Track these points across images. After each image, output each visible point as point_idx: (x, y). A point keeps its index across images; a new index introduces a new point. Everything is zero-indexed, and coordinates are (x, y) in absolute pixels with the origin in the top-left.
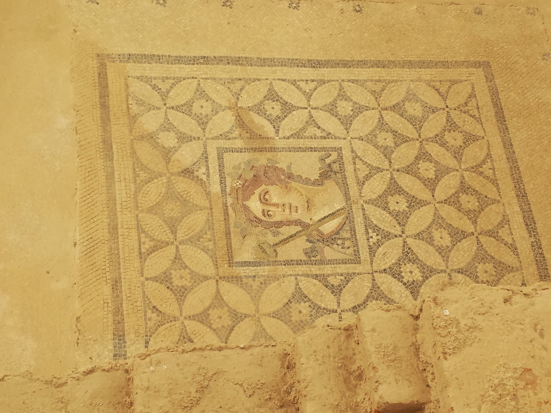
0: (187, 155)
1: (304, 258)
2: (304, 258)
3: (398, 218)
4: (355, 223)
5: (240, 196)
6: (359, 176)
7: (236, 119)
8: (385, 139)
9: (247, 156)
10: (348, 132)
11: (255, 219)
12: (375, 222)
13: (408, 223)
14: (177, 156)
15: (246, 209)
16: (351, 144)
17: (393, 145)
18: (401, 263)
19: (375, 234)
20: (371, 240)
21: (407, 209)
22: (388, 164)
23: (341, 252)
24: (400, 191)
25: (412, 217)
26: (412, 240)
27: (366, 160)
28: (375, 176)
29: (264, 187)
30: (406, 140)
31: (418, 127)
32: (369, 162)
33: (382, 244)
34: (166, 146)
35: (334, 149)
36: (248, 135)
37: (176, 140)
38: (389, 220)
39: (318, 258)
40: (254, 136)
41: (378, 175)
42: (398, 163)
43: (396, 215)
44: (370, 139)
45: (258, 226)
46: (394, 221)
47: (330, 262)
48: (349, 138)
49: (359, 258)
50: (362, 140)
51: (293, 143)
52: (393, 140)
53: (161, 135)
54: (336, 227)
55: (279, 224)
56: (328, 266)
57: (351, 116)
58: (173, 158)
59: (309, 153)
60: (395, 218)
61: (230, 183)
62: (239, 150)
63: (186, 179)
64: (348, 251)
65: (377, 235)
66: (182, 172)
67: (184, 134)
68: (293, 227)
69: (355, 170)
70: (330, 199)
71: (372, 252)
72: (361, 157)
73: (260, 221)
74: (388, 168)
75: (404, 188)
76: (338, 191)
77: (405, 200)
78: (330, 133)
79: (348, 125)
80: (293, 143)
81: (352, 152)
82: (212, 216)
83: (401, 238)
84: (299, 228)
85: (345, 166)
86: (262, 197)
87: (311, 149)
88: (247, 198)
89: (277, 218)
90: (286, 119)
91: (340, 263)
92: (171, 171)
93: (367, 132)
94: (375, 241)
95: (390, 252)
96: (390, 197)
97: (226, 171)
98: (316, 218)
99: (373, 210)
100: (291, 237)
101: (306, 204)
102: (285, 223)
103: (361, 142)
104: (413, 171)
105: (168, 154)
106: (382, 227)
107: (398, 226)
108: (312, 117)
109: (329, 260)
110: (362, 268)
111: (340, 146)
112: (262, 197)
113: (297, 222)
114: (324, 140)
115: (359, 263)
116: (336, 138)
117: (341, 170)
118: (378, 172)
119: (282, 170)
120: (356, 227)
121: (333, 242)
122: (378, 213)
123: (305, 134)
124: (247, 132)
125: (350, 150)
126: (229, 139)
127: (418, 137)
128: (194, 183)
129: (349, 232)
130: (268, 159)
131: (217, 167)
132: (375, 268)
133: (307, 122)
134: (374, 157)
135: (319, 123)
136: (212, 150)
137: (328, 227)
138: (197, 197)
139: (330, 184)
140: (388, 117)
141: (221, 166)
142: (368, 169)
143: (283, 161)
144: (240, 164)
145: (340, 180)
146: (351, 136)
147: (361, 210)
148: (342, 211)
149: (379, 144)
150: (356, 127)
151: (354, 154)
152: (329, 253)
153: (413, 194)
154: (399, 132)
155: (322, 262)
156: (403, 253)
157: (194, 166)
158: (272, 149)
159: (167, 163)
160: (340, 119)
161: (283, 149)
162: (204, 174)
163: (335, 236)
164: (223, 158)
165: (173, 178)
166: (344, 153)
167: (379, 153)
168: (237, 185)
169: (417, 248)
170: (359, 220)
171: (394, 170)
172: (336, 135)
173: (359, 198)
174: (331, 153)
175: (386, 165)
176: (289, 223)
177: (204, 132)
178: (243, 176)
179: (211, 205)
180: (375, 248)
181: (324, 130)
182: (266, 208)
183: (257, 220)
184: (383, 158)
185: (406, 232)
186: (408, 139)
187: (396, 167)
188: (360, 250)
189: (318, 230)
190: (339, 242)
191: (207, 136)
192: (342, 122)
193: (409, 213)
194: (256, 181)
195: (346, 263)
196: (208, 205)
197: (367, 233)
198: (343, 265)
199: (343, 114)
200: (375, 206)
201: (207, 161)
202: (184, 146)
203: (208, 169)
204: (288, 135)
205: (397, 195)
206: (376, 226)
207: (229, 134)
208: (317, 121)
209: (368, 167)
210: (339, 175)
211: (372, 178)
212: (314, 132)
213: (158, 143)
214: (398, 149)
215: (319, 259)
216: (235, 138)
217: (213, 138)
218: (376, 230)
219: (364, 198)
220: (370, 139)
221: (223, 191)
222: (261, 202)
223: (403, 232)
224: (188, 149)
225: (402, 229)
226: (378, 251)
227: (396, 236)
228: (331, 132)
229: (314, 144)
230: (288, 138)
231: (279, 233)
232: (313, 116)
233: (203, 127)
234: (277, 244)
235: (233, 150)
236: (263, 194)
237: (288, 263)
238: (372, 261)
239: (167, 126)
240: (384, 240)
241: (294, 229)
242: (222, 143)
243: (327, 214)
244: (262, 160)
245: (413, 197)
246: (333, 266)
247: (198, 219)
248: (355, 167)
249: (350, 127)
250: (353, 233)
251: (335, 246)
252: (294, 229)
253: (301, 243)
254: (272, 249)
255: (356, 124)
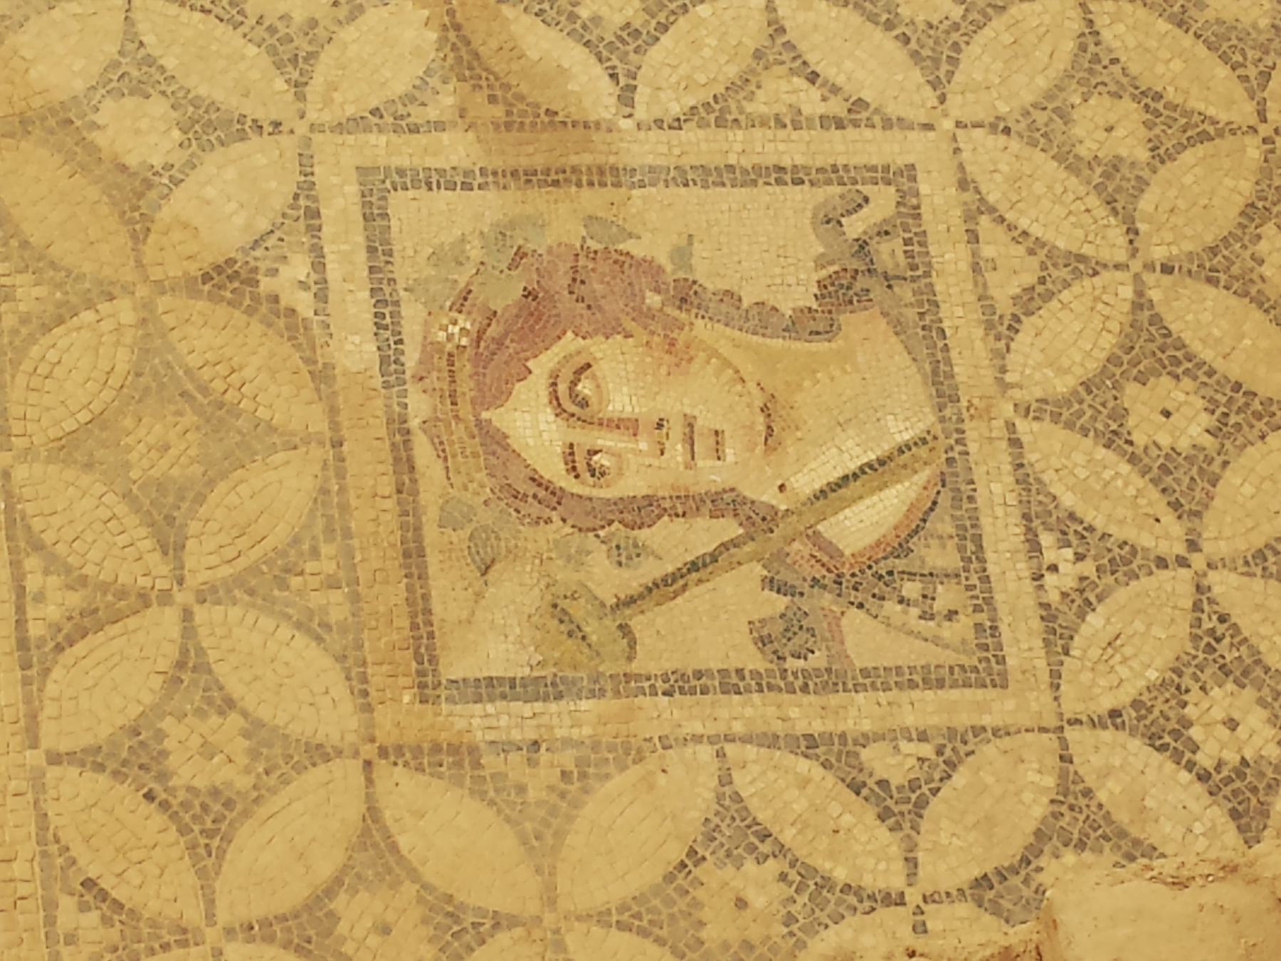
0: (224, 202)
1: (755, 661)
2: (755, 661)
3: (1168, 480)
4: (980, 501)
5: (466, 386)
6: (992, 292)
7: (443, 40)
8: (1109, 129)
9: (491, 206)
10: (942, 99)
11: (532, 489)
12: (1068, 500)
13: (1217, 503)
14: (179, 205)
15: (495, 443)
16: (957, 151)
17: (1143, 155)
18: (1187, 681)
19: (1068, 553)
20: (1050, 579)
21: (1207, 441)
22: (1122, 241)
23: (918, 635)
24: (1176, 362)
25: (1231, 478)
26: (1233, 579)
27: (1024, 223)
28: (1066, 295)
29: (570, 343)
30: (1202, 131)
31: (1252, 72)
32: (1036, 230)
33: (1100, 599)
34: (132, 161)
35: (884, 174)
36: (498, 112)
37: (176, 134)
38: (1131, 491)
39: (818, 660)
40: (523, 114)
41: (1076, 289)
42: (1169, 237)
43: (1162, 469)
44: (1042, 126)
45: (548, 521)
46: (1154, 494)
47: (872, 679)
48: (948, 124)
49: (1001, 661)
50: (1007, 131)
51: (701, 145)
52: (1143, 132)
53: (108, 111)
54: (892, 521)
55: (645, 510)
56: (860, 698)
57: (956, 27)
58: (165, 214)
59: (765, 194)
60: (1155, 482)
61: (417, 328)
62: (459, 179)
63: (222, 311)
64: (948, 631)
65: (1080, 557)
66: (206, 278)
67: (213, 106)
68: (702, 522)
69: (976, 268)
70: (866, 399)
71: (1057, 633)
72: (1003, 208)
73: (556, 496)
74: (1121, 256)
75: (1196, 347)
76: (902, 359)
77: (1200, 403)
78: (860, 103)
79: (945, 67)
80: (701, 145)
81: (963, 184)
82: (341, 475)
83: (1183, 572)
84: (730, 529)
85: (933, 250)
86: (562, 388)
87: (781, 175)
88: (501, 395)
89: (632, 484)
90: (666, 39)
91: (912, 685)
92: (156, 274)
93: (1028, 98)
94: (1070, 584)
95: (1138, 637)
96: (1131, 389)
97: (403, 271)
98: (806, 482)
99: (1058, 447)
100: (694, 566)
101: (761, 419)
102: (667, 504)
103: (1002, 139)
104: (1235, 270)
105: (140, 196)
106: (1099, 523)
107: (1168, 518)
108: (782, 30)
109: (865, 672)
110: (1010, 704)
111: (910, 159)
112: (562, 388)
113: (723, 503)
114: (836, 134)
115: (1001, 683)
116: (888, 124)
117: (914, 267)
118: (1078, 274)
119: (650, 268)
120: (985, 521)
121: (879, 588)
122: (1079, 458)
123: (749, 108)
124: (492, 99)
125: (952, 177)
126: (414, 129)
127: (1253, 120)
128: (256, 328)
129: (951, 545)
130: (590, 220)
131: (362, 256)
132: (1071, 706)
133: (758, 55)
134: (1059, 212)
135: (811, 58)
136: (335, 180)
137: (861, 524)
138: (273, 389)
139: (865, 332)
140: (1120, 28)
141: (379, 251)
142: (1034, 262)
143: (655, 225)
144: (463, 240)
145: (911, 314)
146: (956, 113)
147: (1004, 444)
148: (923, 452)
149: (1082, 151)
150: (978, 76)
151: (968, 196)
152: (866, 637)
153: (1235, 372)
154: (1170, 94)
155: (834, 680)
156: (1195, 638)
157: (259, 253)
158: (607, 175)
159: (138, 238)
160: (907, 40)
161: (654, 176)
162: (303, 285)
163: (891, 561)
164: (385, 216)
165: (163, 303)
166: (924, 189)
167: (1082, 190)
168: (450, 338)
169: (1257, 617)
170: (996, 491)
171: (1150, 267)
172: (893, 110)
173: (993, 390)
174: (867, 189)
175: (1113, 244)
176: (686, 505)
177: (300, 97)
178: (478, 296)
179: (335, 426)
180: (1068, 616)
181: (835, 90)
182: (585, 438)
183: (542, 494)
184: (1101, 211)
185: (1207, 547)
186: (1211, 130)
187: (1159, 254)
188: (1003, 628)
189: (816, 539)
190: (911, 589)
191: (312, 116)
192: (915, 55)
193: (1219, 460)
194: (535, 317)
195: (941, 684)
196: (320, 425)
197: (1034, 547)
198: (929, 694)
199: (920, 19)
200: (1069, 425)
201: (314, 230)
202: (211, 161)
203: (319, 265)
204: (676, 109)
205: (1165, 380)
206: (1072, 516)
207: (412, 109)
208: (802, 46)
209: (1031, 252)
210: (905, 292)
211: (1054, 304)
212: (793, 99)
213: (92, 149)
214: (1163, 171)
215: (823, 664)
216: (439, 126)
217: (339, 128)
218: (1072, 537)
219: (1016, 394)
220: (1042, 126)
221: (390, 361)
222: (560, 410)
223: (1193, 546)
224: (230, 173)
225: (1190, 531)
226: (1085, 629)
227: (1162, 563)
228: (867, 95)
229: (792, 149)
230: (677, 124)
231: (639, 551)
232: (787, 25)
233: (295, 75)
234: (632, 601)
235: (431, 181)
236: (567, 375)
237: (681, 684)
238: (1056, 675)
239: (135, 73)
240: (1109, 579)
241: (705, 534)
242: (380, 147)
243: (853, 466)
244: (562, 221)
245: (1237, 387)
246: (883, 697)
247: (280, 490)
248: (974, 254)
249: (951, 74)
250: (970, 547)
251: (892, 607)
252: (705, 534)
253: (740, 597)
254: (611, 624)
255: (979, 60)
